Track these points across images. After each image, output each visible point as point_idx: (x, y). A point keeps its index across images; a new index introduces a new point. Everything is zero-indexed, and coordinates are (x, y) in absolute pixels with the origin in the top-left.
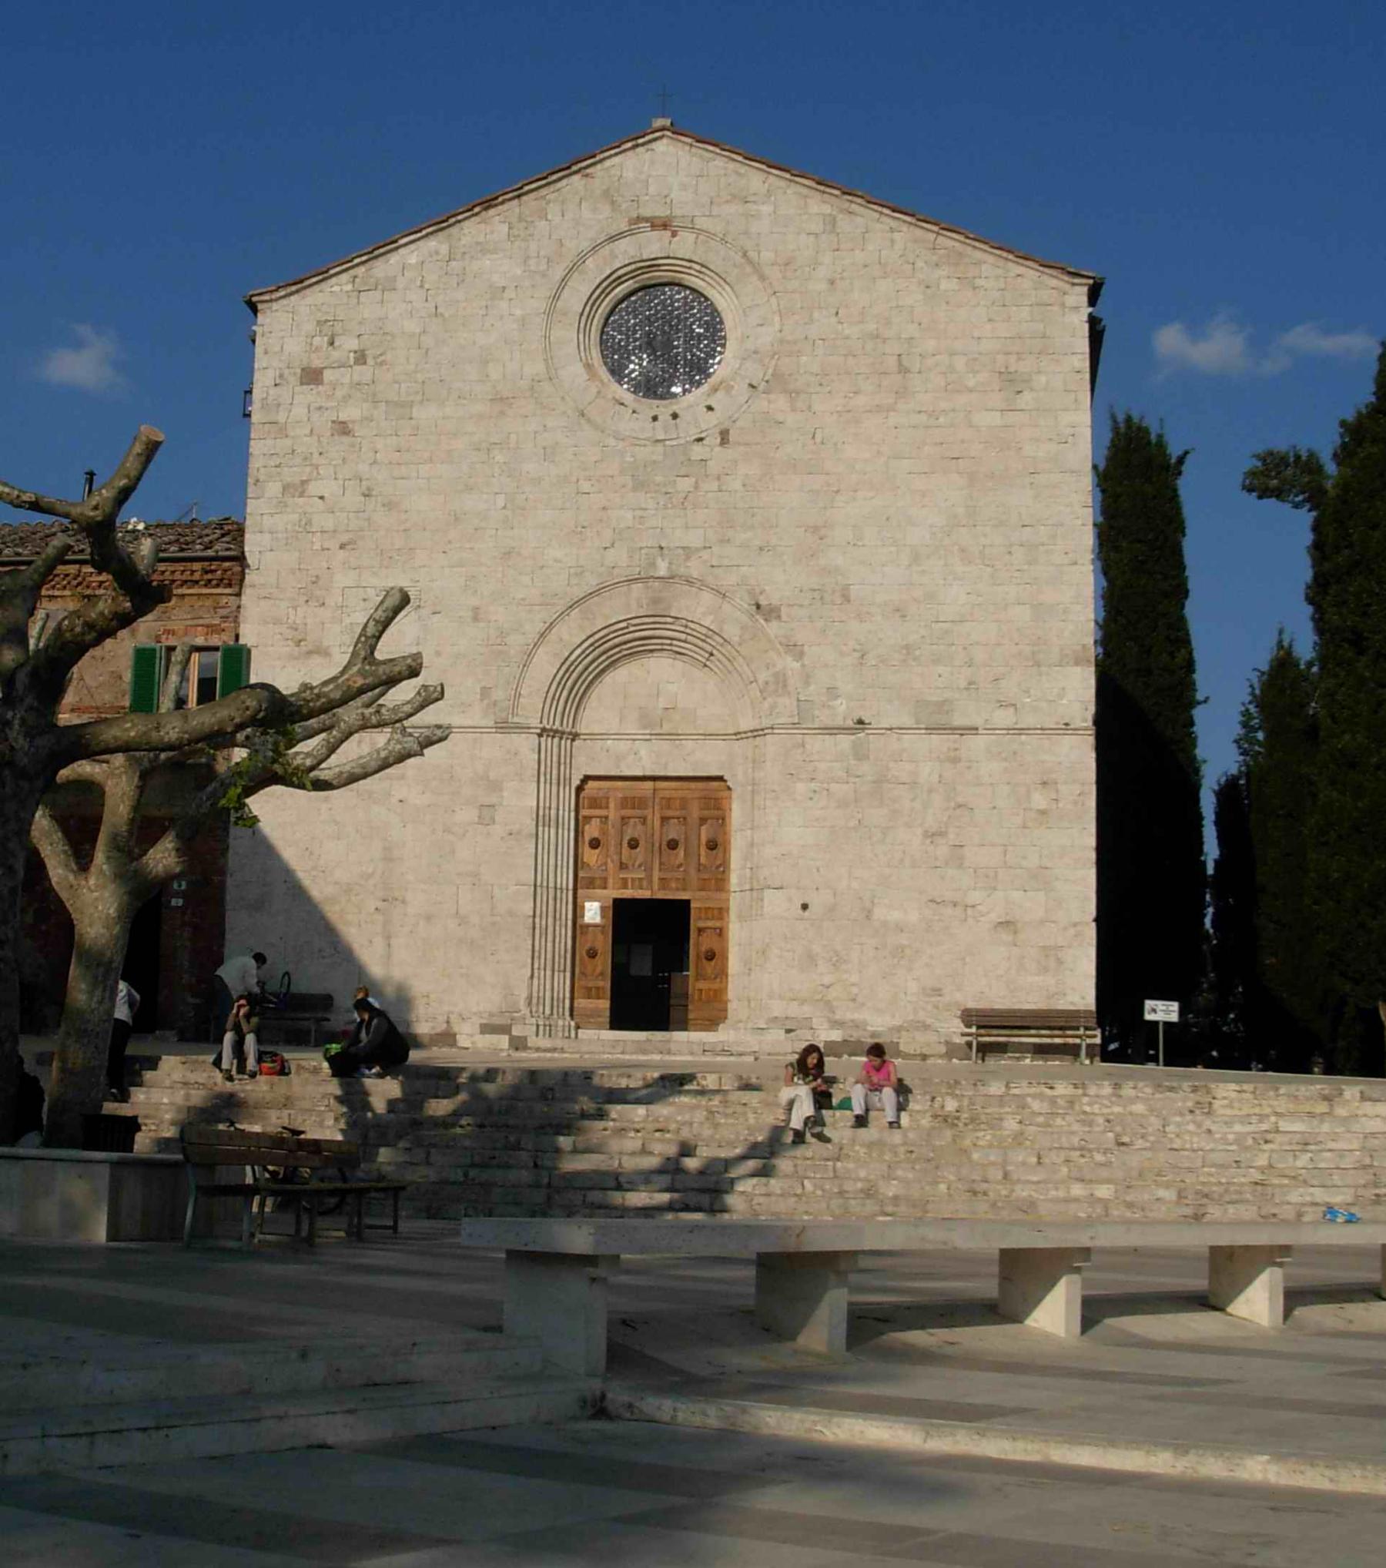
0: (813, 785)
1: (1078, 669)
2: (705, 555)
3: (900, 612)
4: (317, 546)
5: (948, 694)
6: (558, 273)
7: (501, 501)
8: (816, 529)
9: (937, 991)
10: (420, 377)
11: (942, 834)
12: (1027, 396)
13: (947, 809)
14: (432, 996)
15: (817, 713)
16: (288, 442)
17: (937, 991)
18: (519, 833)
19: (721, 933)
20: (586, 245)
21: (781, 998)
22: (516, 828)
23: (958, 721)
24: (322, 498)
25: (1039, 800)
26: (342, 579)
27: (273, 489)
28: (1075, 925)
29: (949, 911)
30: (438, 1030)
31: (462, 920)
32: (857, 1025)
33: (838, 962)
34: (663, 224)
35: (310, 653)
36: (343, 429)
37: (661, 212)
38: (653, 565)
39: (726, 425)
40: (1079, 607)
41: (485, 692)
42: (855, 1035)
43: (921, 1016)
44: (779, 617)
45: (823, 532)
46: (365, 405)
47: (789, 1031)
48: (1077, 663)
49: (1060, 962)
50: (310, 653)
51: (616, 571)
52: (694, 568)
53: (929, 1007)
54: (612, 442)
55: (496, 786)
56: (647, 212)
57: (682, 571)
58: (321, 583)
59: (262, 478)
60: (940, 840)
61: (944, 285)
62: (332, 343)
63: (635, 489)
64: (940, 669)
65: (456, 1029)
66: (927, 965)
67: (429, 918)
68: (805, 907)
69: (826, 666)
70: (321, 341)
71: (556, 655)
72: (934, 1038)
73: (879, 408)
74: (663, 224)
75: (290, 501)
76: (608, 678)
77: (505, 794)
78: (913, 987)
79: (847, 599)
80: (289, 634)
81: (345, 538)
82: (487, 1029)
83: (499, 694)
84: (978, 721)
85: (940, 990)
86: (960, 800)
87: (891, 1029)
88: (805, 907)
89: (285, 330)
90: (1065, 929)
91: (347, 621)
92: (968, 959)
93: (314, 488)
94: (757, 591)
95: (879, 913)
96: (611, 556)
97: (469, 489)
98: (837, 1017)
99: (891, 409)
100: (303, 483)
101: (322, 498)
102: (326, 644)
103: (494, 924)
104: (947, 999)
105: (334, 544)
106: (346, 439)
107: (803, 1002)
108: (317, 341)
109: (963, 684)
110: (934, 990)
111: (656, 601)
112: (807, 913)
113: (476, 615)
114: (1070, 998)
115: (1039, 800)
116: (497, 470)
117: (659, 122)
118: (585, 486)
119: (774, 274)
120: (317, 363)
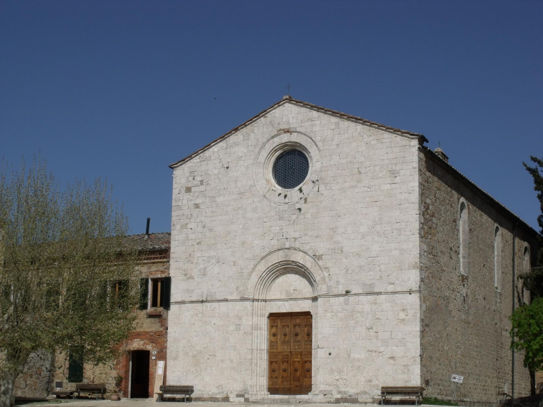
0: (332, 314)
1: (414, 271)
2: (300, 240)
3: (359, 255)
4: (190, 244)
5: (373, 281)
6: (257, 150)
8: (333, 229)
9: (370, 381)
10: (218, 188)
11: (372, 328)
12: (398, 178)
16: (182, 211)
17: (370, 381)
18: (247, 332)
20: (265, 140)
21: (323, 384)
22: (246, 331)
23: (377, 290)
25: (402, 315)
26: (198, 254)
27: (178, 227)
28: (414, 357)
29: (374, 354)
30: (224, 396)
31: (232, 361)
32: (345, 393)
33: (340, 372)
34: (287, 131)
35: (189, 278)
36: (197, 206)
37: (286, 127)
38: (285, 244)
40: (414, 249)
42: (345, 396)
43: (366, 389)
45: (335, 229)
46: (203, 198)
47: (325, 395)
48: (414, 269)
49: (408, 370)
50: (189, 278)
51: (274, 247)
52: (297, 245)
53: (368, 386)
54: (272, 205)
55: (240, 318)
56: (282, 128)
57: (293, 245)
59: (175, 223)
60: (371, 330)
62: (194, 179)
63: (280, 220)
64: (371, 273)
65: (229, 396)
66: (367, 372)
67: (222, 361)
68: (330, 354)
69: (336, 274)
70: (191, 178)
71: (257, 275)
72: (368, 396)
73: (353, 187)
74: (287, 131)
77: (243, 320)
78: (363, 379)
79: (342, 251)
80: (183, 272)
81: (198, 241)
82: (238, 396)
83: (241, 289)
84: (382, 290)
86: (377, 317)
87: (355, 394)
88: (330, 354)
89: (181, 175)
90: (410, 359)
91: (199, 267)
93: (189, 226)
95: (352, 355)
97: (232, 223)
98: (340, 390)
99: (356, 186)
100: (187, 224)
102: (193, 275)
103: (240, 362)
104: (373, 383)
105: (195, 243)
106: (197, 209)
107: (330, 385)
109: (378, 278)
111: (286, 256)
112: (331, 356)
113: (235, 264)
114: (412, 382)
115: (402, 315)
116: (240, 217)
117: (285, 97)
118: (265, 220)
119: (320, 144)
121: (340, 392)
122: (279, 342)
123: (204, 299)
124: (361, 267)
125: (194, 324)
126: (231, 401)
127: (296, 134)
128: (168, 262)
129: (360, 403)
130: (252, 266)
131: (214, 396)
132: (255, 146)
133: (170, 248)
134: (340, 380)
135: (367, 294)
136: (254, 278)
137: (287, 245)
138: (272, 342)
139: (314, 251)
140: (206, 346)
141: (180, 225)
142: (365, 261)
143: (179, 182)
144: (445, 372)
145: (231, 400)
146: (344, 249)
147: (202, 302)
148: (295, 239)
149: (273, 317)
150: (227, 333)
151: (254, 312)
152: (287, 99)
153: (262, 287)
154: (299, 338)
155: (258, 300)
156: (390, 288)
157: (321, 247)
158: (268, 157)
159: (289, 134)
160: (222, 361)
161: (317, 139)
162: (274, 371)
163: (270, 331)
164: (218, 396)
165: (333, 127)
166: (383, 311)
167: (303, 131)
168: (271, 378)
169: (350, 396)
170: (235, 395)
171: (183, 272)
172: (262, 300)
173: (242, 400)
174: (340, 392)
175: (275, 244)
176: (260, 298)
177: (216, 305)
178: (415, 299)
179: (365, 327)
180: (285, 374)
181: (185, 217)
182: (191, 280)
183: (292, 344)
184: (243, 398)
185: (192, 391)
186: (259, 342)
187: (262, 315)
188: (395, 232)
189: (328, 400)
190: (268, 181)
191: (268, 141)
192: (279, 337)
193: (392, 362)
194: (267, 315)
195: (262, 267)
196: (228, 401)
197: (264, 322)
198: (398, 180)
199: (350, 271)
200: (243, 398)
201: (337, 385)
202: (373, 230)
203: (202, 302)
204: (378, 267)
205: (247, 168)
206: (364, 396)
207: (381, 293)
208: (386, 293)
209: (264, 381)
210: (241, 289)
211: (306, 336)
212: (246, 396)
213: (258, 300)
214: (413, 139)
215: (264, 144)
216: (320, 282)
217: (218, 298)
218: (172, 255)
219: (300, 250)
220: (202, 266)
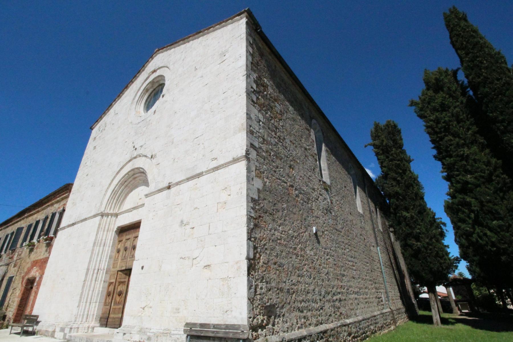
17: (178, 310)
23: (198, 171)
68: (142, 268)
76: (131, 195)
79: (173, 143)
86: (195, 206)
88: (142, 268)
130: (110, 182)
133: (72, 184)
135: (188, 179)
144: (312, 287)
147: (73, 224)
153: (115, 201)
155: (107, 215)
156: (214, 164)
158: (141, 96)
162: (109, 294)
172: (112, 215)
176: (111, 212)
178: (242, 167)
185: (38, 323)
186: (99, 259)
193: (207, 273)
197: (111, 236)
199: (176, 160)
203: (73, 224)
207: (203, 172)
208: (208, 172)
213: (107, 215)
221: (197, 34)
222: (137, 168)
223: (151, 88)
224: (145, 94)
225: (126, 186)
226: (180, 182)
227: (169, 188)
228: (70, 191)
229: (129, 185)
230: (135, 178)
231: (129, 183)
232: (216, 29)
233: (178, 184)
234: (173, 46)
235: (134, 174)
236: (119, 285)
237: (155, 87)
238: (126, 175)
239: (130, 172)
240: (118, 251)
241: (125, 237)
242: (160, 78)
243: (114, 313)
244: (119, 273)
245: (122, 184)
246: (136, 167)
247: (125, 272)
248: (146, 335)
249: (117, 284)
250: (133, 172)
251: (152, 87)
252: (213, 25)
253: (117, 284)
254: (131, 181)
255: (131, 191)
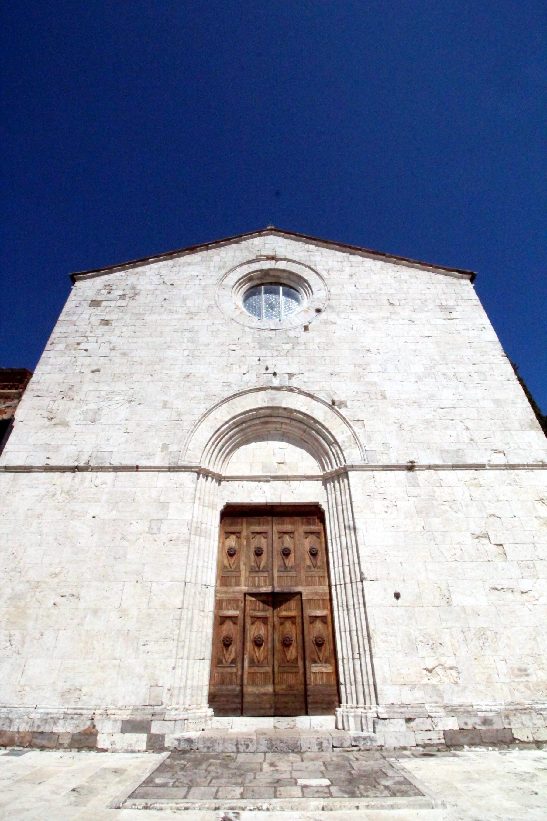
0: (386, 503)
2: (300, 376)
5: (459, 446)
7: (186, 353)
8: (360, 366)
9: (523, 672)
13: (482, 518)
14: (85, 690)
15: (379, 457)
16: (76, 327)
17: (523, 672)
18: (178, 539)
19: (328, 621)
21: (393, 684)
22: (175, 536)
24: (86, 350)
26: (87, 387)
27: (61, 346)
29: (509, 595)
30: (82, 728)
31: (123, 613)
32: (469, 712)
33: (435, 645)
34: (273, 258)
36: (106, 322)
37: (271, 253)
38: (271, 381)
39: (306, 324)
41: (165, 447)
42: (471, 722)
43: (518, 697)
44: (346, 406)
45: (364, 367)
46: (120, 314)
47: (409, 720)
52: (295, 383)
53: (522, 688)
54: (248, 329)
55: (164, 506)
56: (263, 253)
57: (287, 384)
58: (74, 389)
59: (55, 342)
61: (402, 277)
63: (260, 348)
64: (449, 432)
65: (99, 727)
66: (508, 646)
69: (380, 431)
70: (104, 292)
71: (212, 427)
74: (273, 258)
75: (68, 352)
76: (243, 448)
77: (170, 511)
78: (502, 667)
79: (384, 397)
80: (46, 414)
81: (95, 368)
83: (173, 448)
84: (484, 461)
85: (525, 670)
88: (397, 596)
89: (85, 288)
91: (85, 408)
92: (539, 640)
93: (81, 347)
94: (332, 393)
95: (456, 599)
96: (246, 378)
98: (446, 702)
99: (388, 318)
100: (78, 344)
101: (86, 350)
102: (67, 419)
103: (149, 615)
105: (87, 371)
106: (106, 327)
107: (413, 687)
108: (103, 291)
109: (467, 441)
110: (520, 670)
116: (186, 340)
117: (269, 227)
118: (233, 347)
119: (324, 274)
120: (99, 298)
121: (452, 711)
122: (242, 567)
123: (82, 464)
124: (427, 422)
125: (39, 516)
126: (100, 745)
127: (285, 262)
128: (19, 396)
129: (523, 745)
131: (46, 729)
132: (220, 268)
134: (438, 670)
135: (455, 467)
136: (206, 431)
137: (276, 382)
138: (225, 567)
139: (328, 395)
140: (57, 571)
141: (64, 345)
142: (433, 413)
143: (81, 294)
145: (102, 741)
146: (387, 394)
147: (74, 469)
148: (291, 375)
149: (232, 514)
150: (123, 538)
151: (198, 495)
152: (272, 230)
154: (290, 561)
156: (499, 459)
157: (342, 391)
159: (274, 261)
160: (95, 612)
161: (319, 268)
162: (227, 643)
163: (223, 543)
164: (59, 729)
165: (340, 260)
166: (498, 501)
167: (297, 259)
168: (217, 662)
169: (486, 721)
170: (119, 725)
171: (46, 414)
173: (140, 740)
174: (452, 711)
175: (252, 381)
177: (109, 476)
179: (468, 534)
180: (260, 654)
181: (78, 334)
182: (60, 428)
183: (276, 574)
184: (145, 736)
187: (213, 507)
188: (475, 376)
189: (422, 738)
190: (237, 307)
191: (241, 265)
192: (243, 558)
194: (221, 507)
195: (224, 414)
196: (92, 747)
198: (453, 316)
200: (145, 736)
201: (434, 686)
202: (433, 371)
203: (74, 469)
204: (461, 424)
205: (205, 288)
206: (525, 719)
209: (199, 674)
210: (173, 448)
211: (307, 556)
212: (156, 728)
213: (207, 474)
214: (462, 278)
215: (235, 268)
216: (347, 444)
217: (116, 463)
218: (30, 386)
219: (301, 392)
220: (93, 406)
221: (373, 253)
222: (285, 409)
223: (259, 278)
224: (245, 282)
225: (242, 430)
226: (438, 466)
227: (411, 467)
228: (24, 388)
229: (248, 430)
230: (266, 423)
231: (249, 427)
232: (413, 267)
233: (429, 467)
234: (315, 242)
235: (271, 416)
236: (253, 624)
237: (265, 281)
238: (251, 410)
239: (261, 408)
240: (231, 553)
241: (246, 528)
242: (285, 275)
243: (253, 683)
244: (248, 598)
245: (237, 425)
246: (284, 405)
247: (263, 598)
248: (476, 715)
249: (248, 620)
250: (268, 412)
251: (260, 278)
252: (411, 260)
253: (248, 620)
254: (255, 425)
255: (247, 441)
